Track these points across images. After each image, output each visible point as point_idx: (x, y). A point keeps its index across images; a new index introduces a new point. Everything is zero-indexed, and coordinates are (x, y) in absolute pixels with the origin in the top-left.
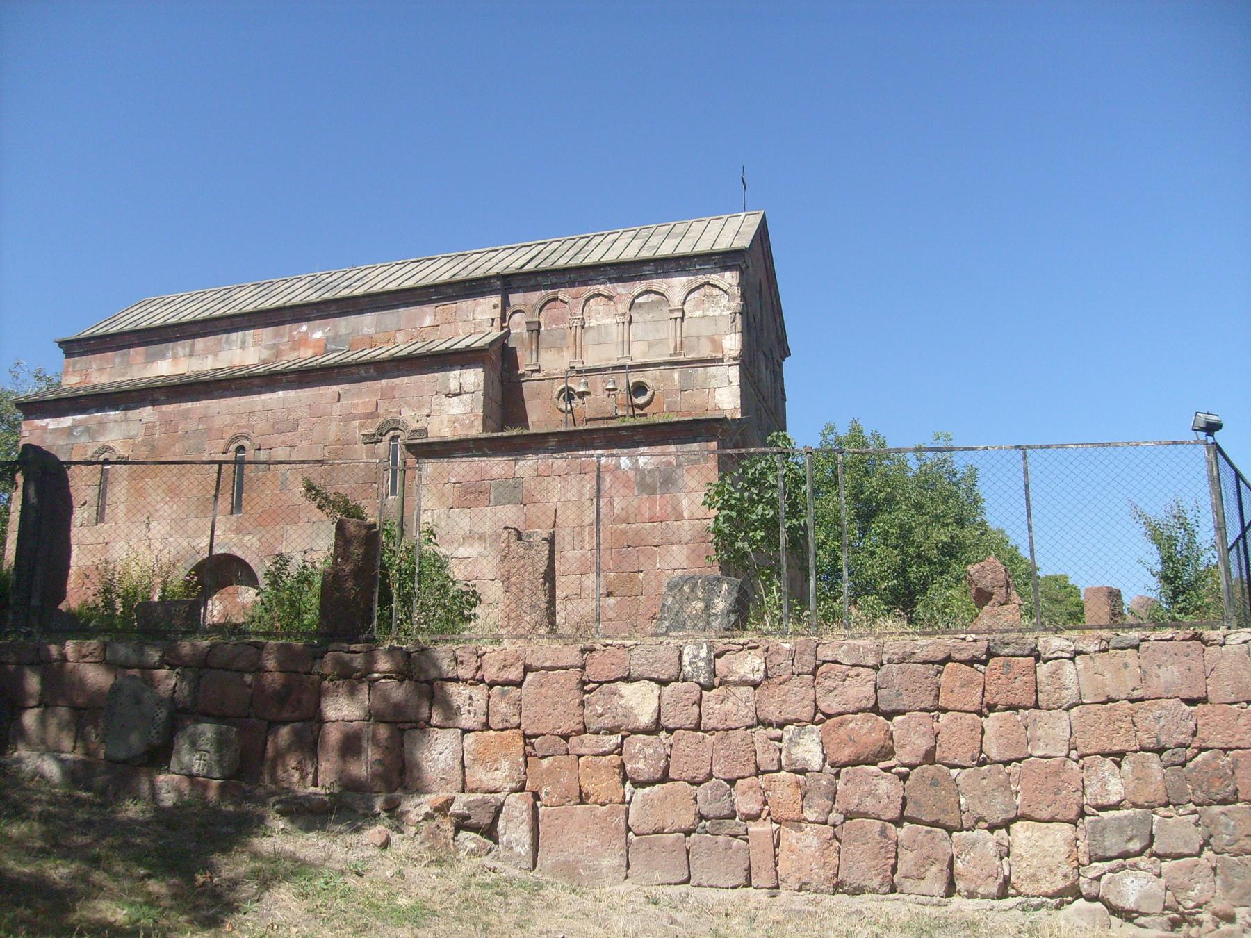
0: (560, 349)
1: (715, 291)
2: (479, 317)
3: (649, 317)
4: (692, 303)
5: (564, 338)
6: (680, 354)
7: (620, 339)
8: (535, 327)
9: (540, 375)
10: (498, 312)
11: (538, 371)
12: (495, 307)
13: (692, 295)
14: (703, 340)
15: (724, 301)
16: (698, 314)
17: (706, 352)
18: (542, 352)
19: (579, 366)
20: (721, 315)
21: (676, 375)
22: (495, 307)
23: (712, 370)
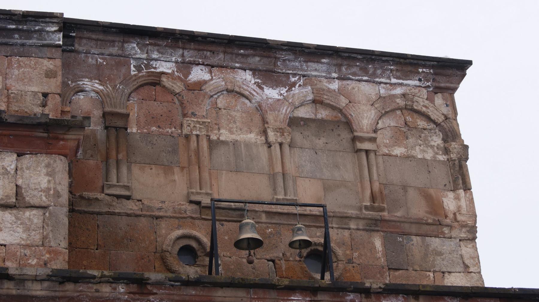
0: (168, 169)
1: (422, 123)
2: (16, 87)
3: (320, 142)
4: (388, 133)
5: (175, 151)
6: (382, 210)
7: (278, 168)
8: (120, 123)
9: (131, 206)
10: (53, 85)
11: (128, 198)
12: (50, 74)
13: (389, 122)
14: (412, 194)
15: (437, 140)
16: (398, 151)
17: (418, 210)
18: (136, 170)
19: (206, 201)
20: (434, 160)
21: (378, 243)
22: (50, 74)
23: (435, 243)
